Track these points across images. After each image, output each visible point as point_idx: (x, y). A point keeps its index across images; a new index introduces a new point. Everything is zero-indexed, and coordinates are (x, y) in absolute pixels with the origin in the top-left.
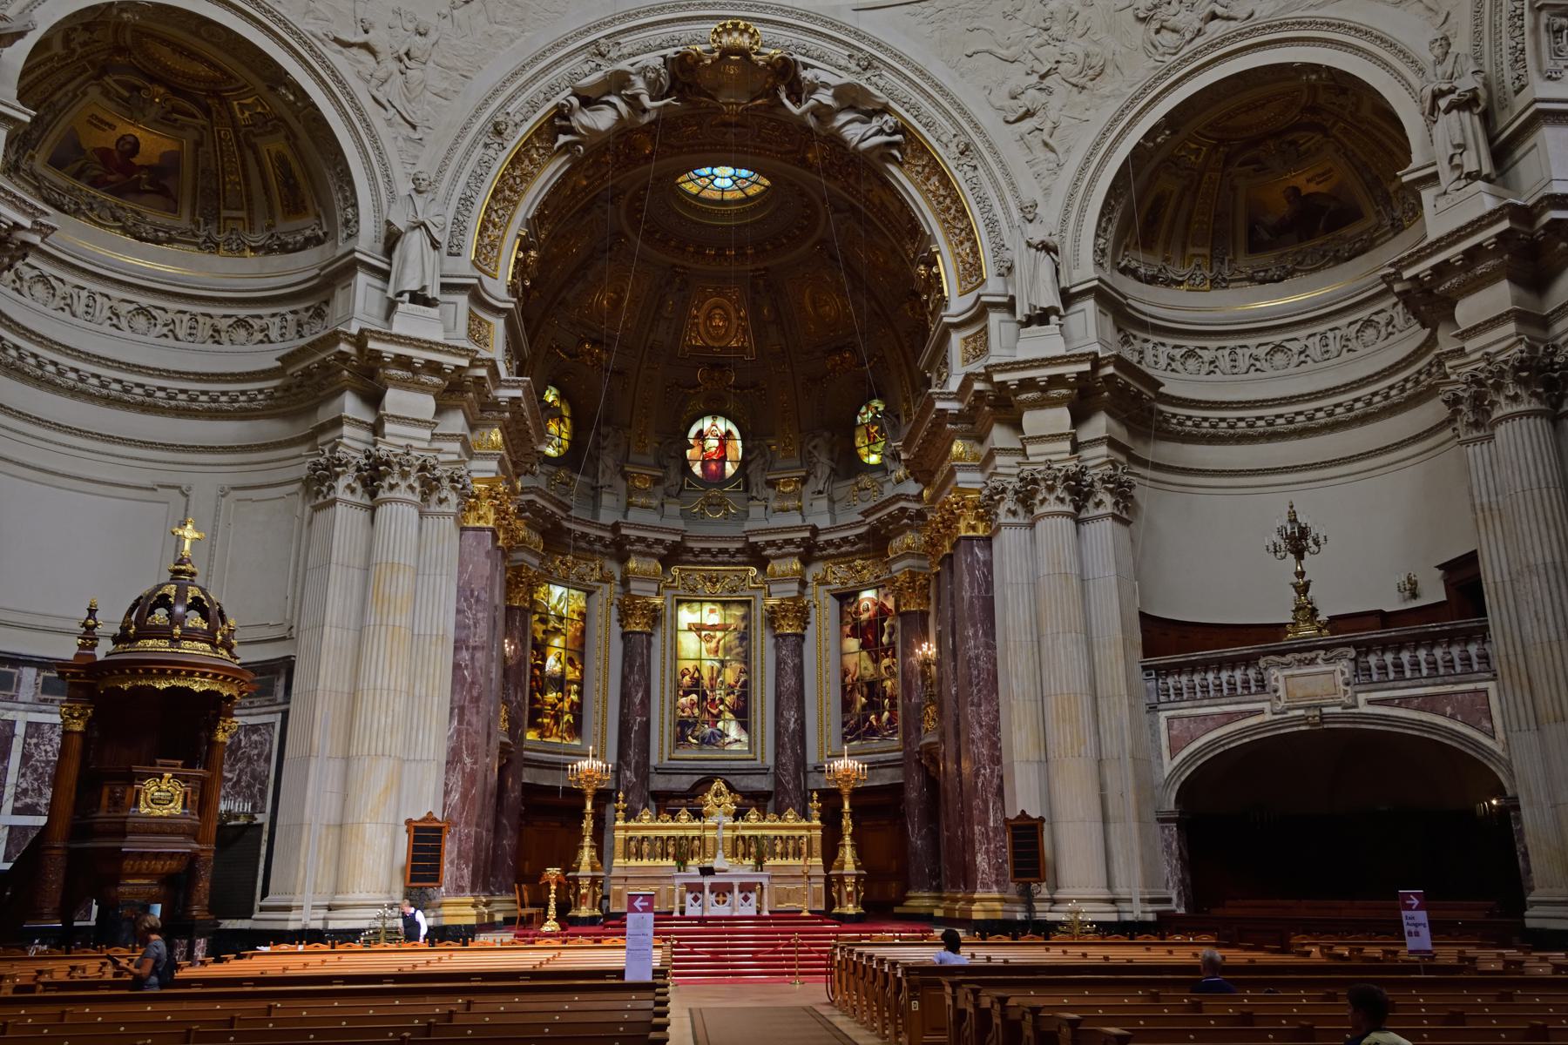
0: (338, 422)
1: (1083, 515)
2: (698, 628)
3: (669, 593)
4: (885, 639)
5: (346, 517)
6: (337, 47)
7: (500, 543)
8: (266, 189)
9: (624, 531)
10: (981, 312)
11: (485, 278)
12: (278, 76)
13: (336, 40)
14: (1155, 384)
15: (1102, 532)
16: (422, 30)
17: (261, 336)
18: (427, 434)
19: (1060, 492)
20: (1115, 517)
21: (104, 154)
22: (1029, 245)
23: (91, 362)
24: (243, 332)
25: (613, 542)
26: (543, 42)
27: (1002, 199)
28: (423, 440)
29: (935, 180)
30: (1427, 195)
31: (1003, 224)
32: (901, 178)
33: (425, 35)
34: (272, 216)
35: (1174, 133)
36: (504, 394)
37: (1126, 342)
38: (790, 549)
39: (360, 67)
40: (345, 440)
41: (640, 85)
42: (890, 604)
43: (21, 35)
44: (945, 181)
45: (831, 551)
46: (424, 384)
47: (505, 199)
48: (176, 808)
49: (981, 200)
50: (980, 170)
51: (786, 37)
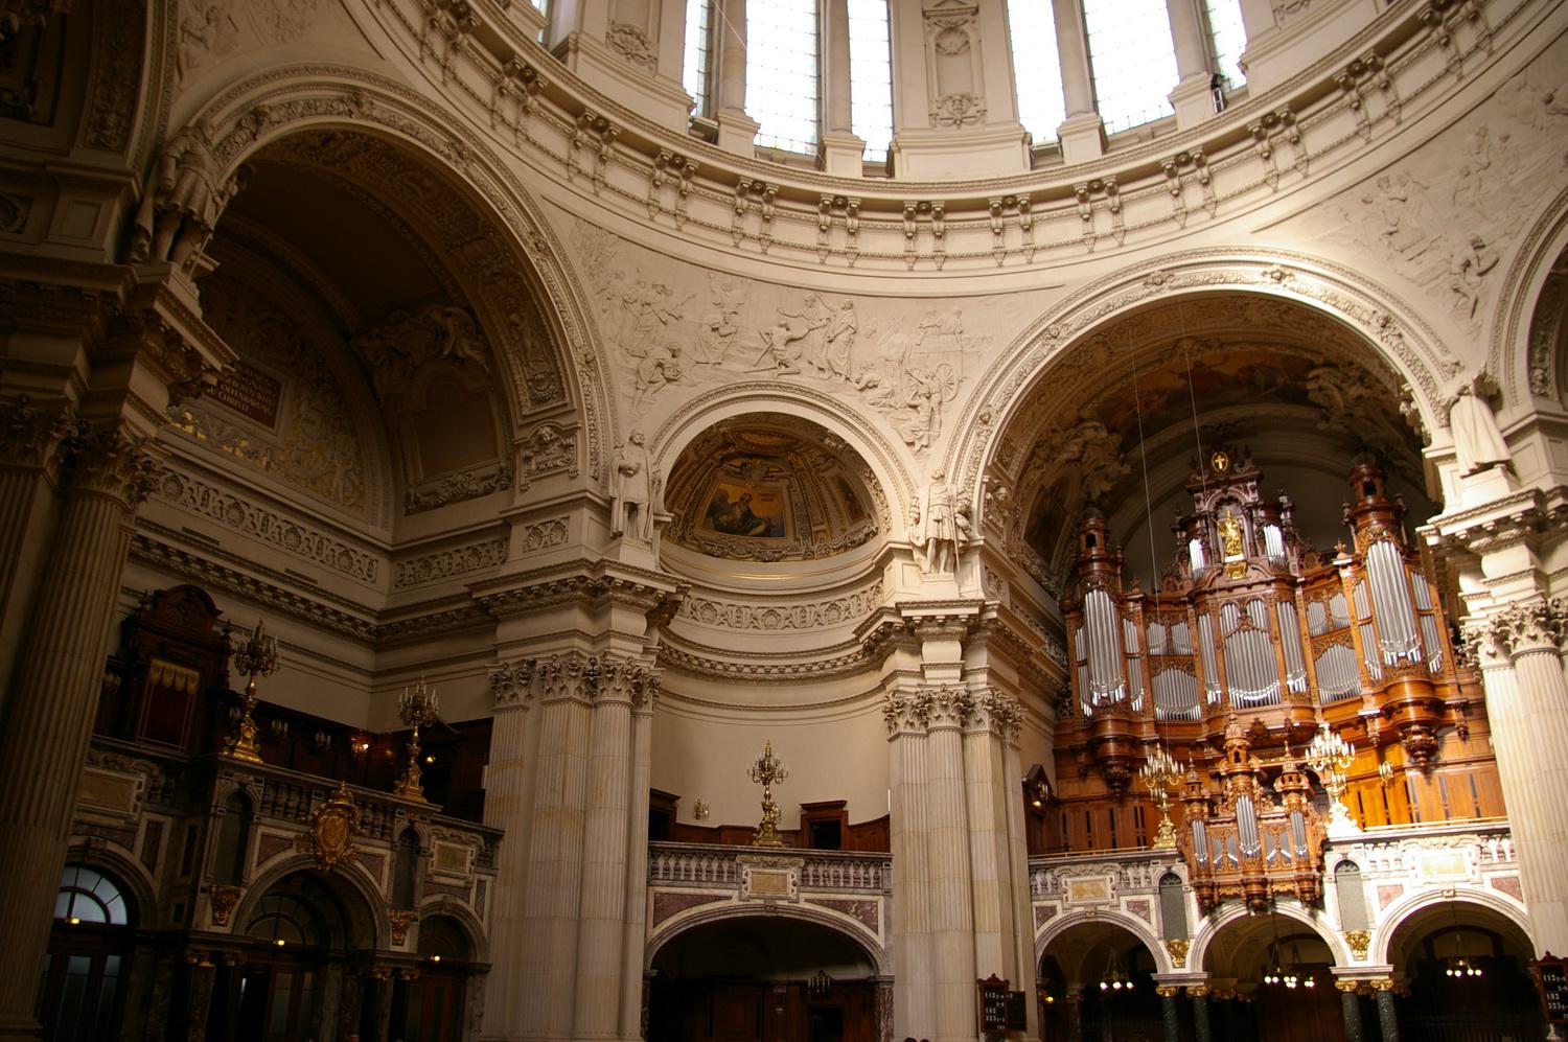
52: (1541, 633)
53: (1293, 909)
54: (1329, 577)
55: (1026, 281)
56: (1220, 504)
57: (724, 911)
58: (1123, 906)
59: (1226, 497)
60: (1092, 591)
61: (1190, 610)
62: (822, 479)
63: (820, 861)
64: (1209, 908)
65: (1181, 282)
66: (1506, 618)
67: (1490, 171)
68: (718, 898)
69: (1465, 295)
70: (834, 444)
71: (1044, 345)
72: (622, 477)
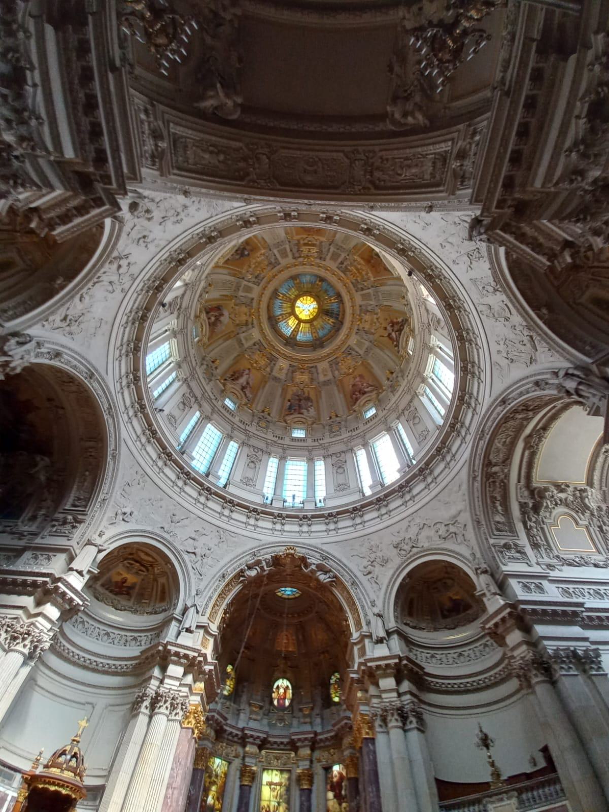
0: (150, 678)
1: (407, 728)
2: (270, 784)
3: (260, 764)
4: (343, 792)
5: (142, 719)
7: (195, 736)
8: (157, 592)
9: (246, 732)
10: (363, 637)
11: (211, 624)
14: (422, 668)
15: (414, 735)
18: (177, 683)
19: (396, 717)
20: (419, 729)
21: (117, 582)
22: (374, 614)
24: (134, 642)
25: (242, 737)
26: (240, 551)
27: (365, 598)
29: (345, 592)
30: (485, 599)
31: (366, 607)
32: (336, 592)
35: (411, 579)
36: (207, 668)
37: (410, 651)
38: (307, 743)
40: (151, 686)
41: (264, 563)
42: (344, 773)
43: (105, 550)
44: (348, 592)
45: (322, 744)
49: (359, 599)
50: (358, 590)
51: (304, 551)
71: (86, 373)
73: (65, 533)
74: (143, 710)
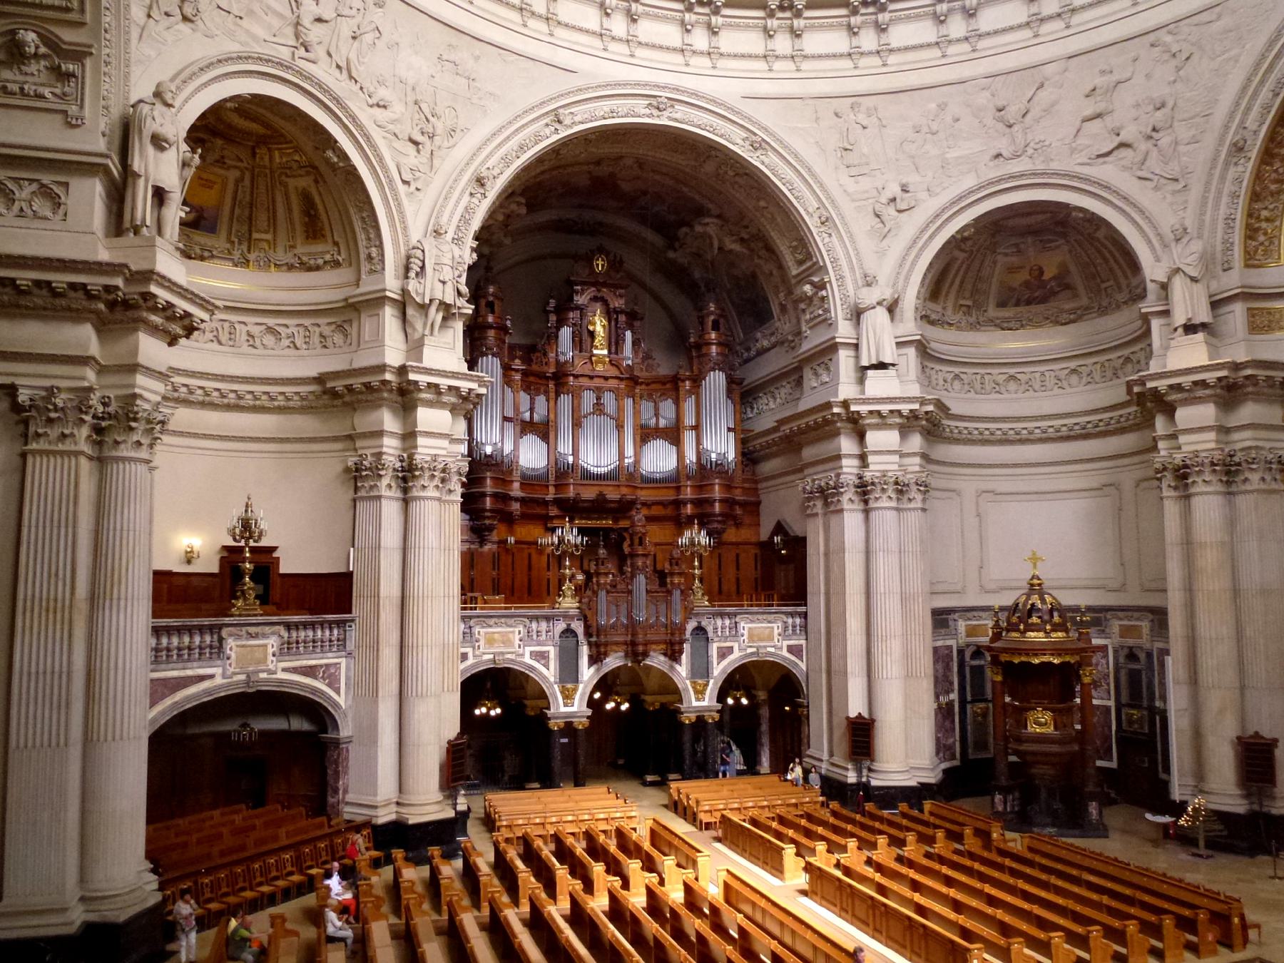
5: (1171, 509)
6: (1101, 160)
12: (1066, 206)
13: (1099, 156)
16: (1158, 106)
17: (1137, 367)
21: (1027, 284)
23: (1045, 420)
24: (1129, 366)
28: (1209, 441)
33: (1163, 105)
34: (1127, 277)
39: (1124, 162)
46: (1200, 397)
47: (1272, 194)
48: (1050, 730)
52: (894, 496)
53: (657, 660)
54: (664, 384)
55: (544, 52)
56: (595, 299)
57: (207, 692)
58: (527, 655)
59: (599, 295)
60: (487, 355)
61: (551, 385)
62: (286, 186)
63: (297, 626)
64: (595, 659)
65: (678, 116)
66: (876, 481)
67: (935, 137)
68: (202, 678)
69: (883, 223)
70: (336, 160)
71: (547, 125)
72: (150, 150)
73: (820, 315)
74: (1167, 492)
